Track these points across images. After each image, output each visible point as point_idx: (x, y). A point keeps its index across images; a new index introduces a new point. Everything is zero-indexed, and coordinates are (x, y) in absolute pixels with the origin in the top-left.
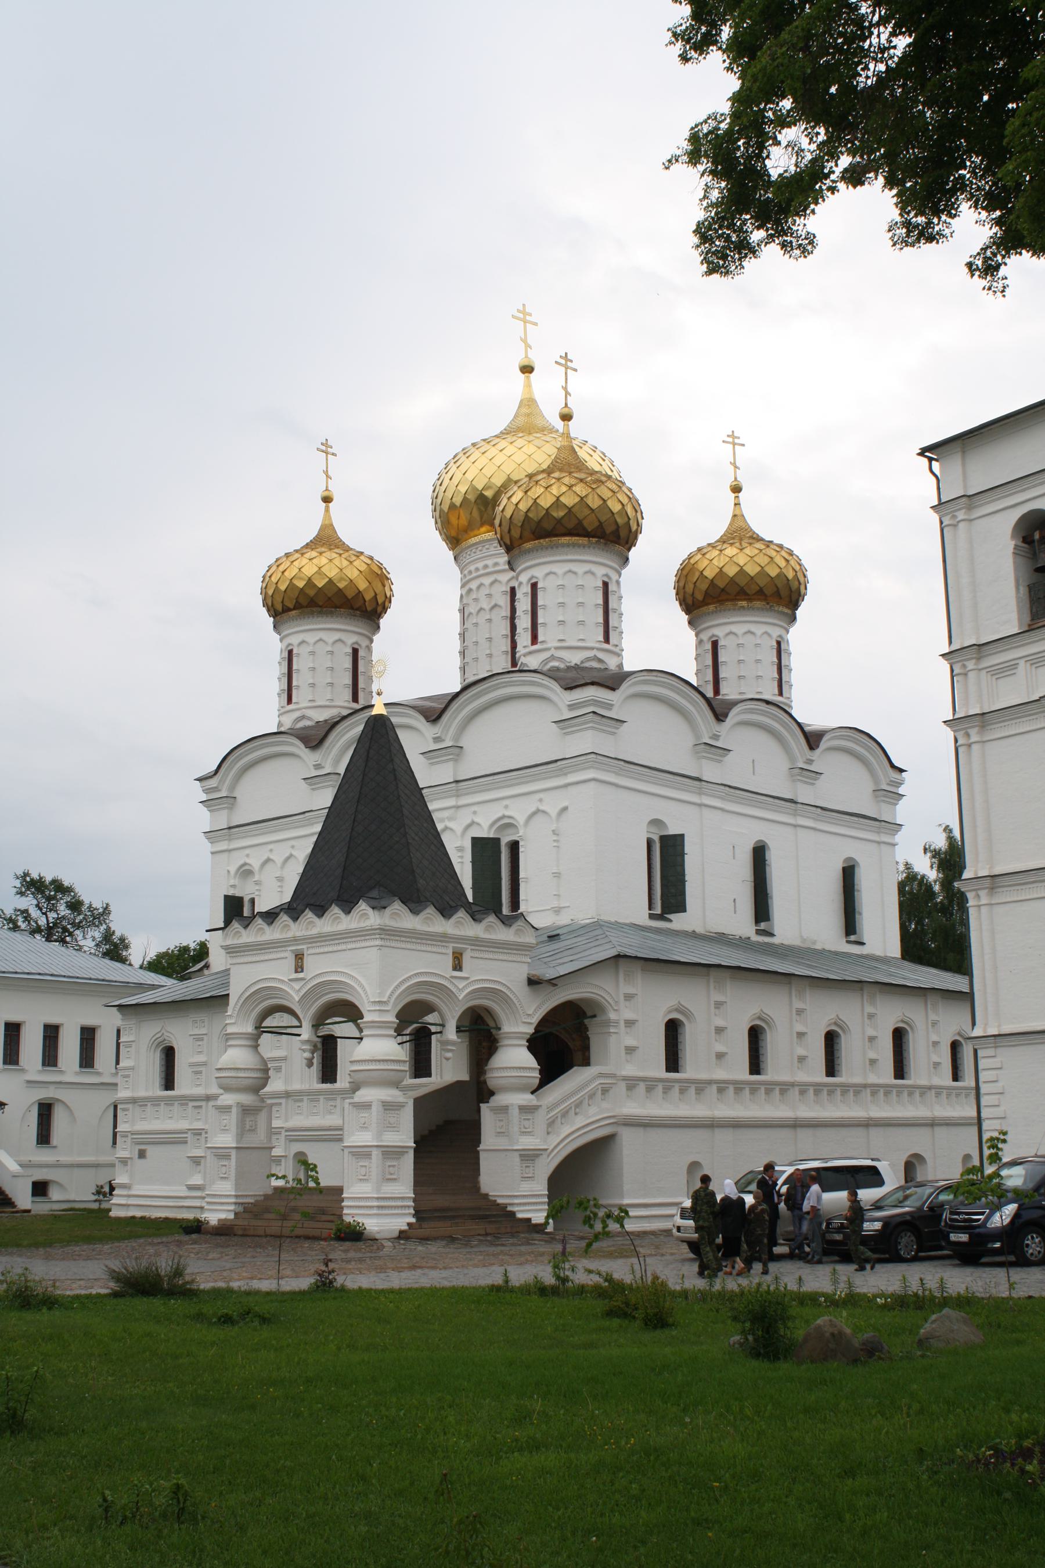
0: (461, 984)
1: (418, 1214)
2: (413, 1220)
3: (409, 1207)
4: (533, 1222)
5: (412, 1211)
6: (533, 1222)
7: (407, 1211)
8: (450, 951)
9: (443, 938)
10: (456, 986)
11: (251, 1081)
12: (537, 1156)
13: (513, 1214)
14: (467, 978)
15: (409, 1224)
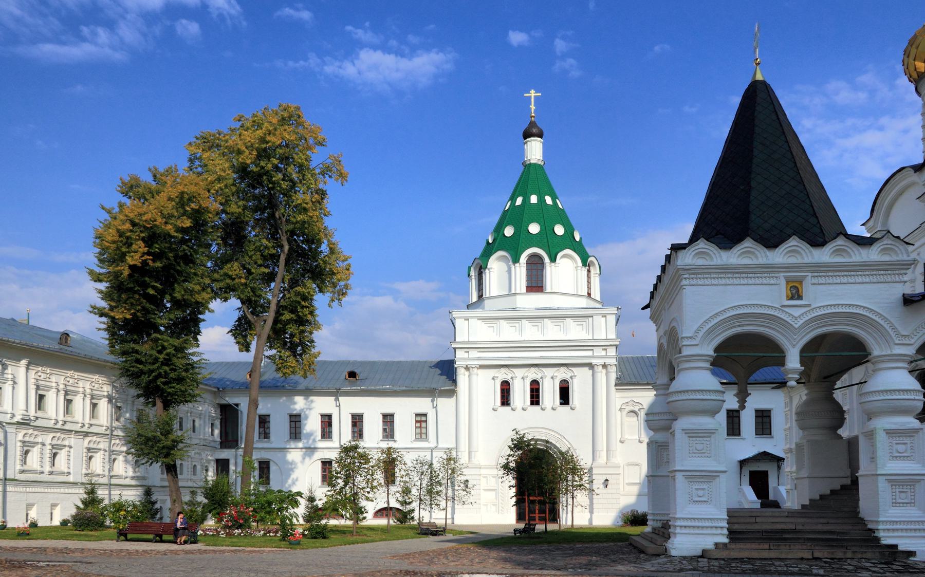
0: (797, 312)
1: (734, 535)
2: (726, 540)
3: (722, 528)
4: (900, 548)
5: (725, 532)
6: (900, 548)
7: (719, 531)
8: (783, 282)
9: (770, 269)
10: (790, 315)
11: (663, 422)
12: (919, 481)
13: (877, 539)
14: (809, 306)
15: (716, 544)
